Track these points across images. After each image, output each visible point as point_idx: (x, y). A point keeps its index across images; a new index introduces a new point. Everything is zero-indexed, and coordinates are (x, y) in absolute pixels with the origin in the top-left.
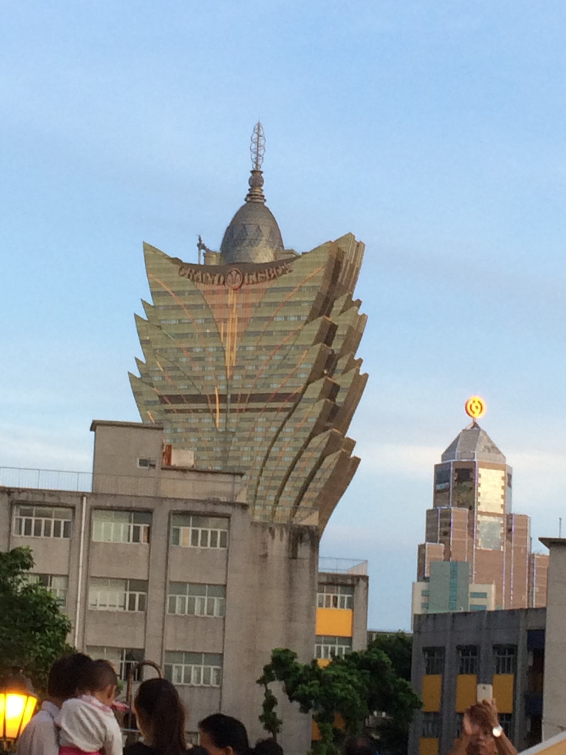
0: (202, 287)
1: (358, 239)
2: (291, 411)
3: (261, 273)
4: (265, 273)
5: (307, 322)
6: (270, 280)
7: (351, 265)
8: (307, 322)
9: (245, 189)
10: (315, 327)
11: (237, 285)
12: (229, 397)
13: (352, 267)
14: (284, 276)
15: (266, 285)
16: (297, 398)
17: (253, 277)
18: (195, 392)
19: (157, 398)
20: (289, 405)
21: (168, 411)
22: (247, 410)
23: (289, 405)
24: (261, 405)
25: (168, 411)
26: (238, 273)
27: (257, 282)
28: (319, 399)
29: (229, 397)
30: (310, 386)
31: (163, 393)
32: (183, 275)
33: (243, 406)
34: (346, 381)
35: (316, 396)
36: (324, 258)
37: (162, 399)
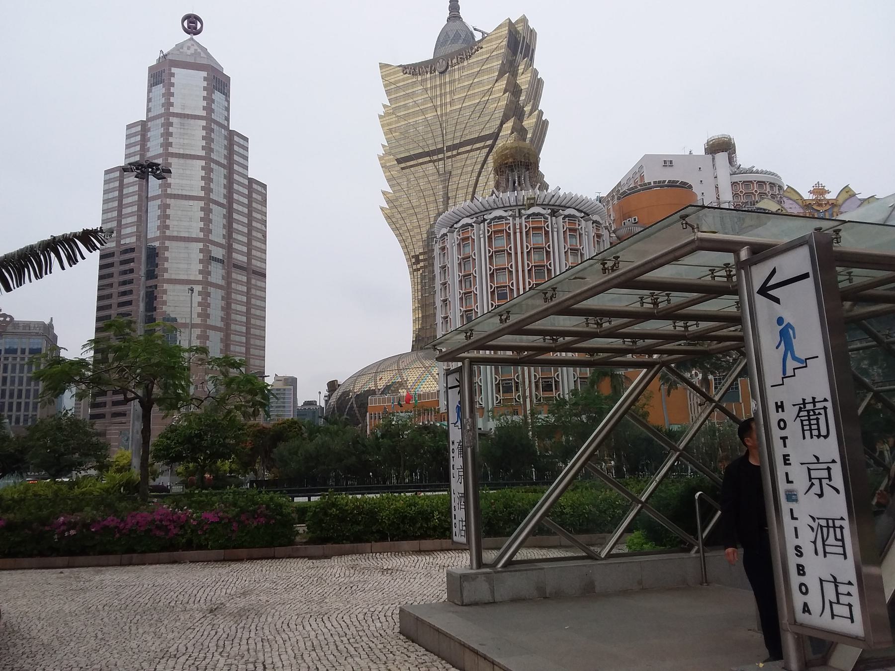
0: (420, 78)
1: (531, 25)
2: (492, 147)
3: (460, 55)
4: (463, 55)
5: (496, 81)
6: (467, 59)
7: (528, 56)
8: (496, 81)
9: (447, 14)
10: (502, 84)
11: (444, 68)
12: (445, 149)
13: (528, 46)
14: (477, 52)
15: (465, 63)
16: (495, 136)
17: (455, 61)
18: (421, 151)
19: (396, 162)
20: (489, 142)
21: (403, 169)
22: (459, 154)
23: (489, 142)
24: (469, 148)
25: (403, 169)
26: (443, 60)
27: (458, 64)
28: (512, 133)
29: (445, 149)
30: (504, 126)
31: (399, 156)
32: (406, 73)
33: (455, 152)
34: (531, 121)
35: (509, 132)
36: (505, 31)
37: (399, 161)
